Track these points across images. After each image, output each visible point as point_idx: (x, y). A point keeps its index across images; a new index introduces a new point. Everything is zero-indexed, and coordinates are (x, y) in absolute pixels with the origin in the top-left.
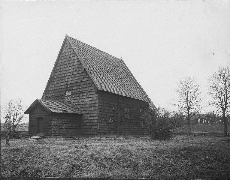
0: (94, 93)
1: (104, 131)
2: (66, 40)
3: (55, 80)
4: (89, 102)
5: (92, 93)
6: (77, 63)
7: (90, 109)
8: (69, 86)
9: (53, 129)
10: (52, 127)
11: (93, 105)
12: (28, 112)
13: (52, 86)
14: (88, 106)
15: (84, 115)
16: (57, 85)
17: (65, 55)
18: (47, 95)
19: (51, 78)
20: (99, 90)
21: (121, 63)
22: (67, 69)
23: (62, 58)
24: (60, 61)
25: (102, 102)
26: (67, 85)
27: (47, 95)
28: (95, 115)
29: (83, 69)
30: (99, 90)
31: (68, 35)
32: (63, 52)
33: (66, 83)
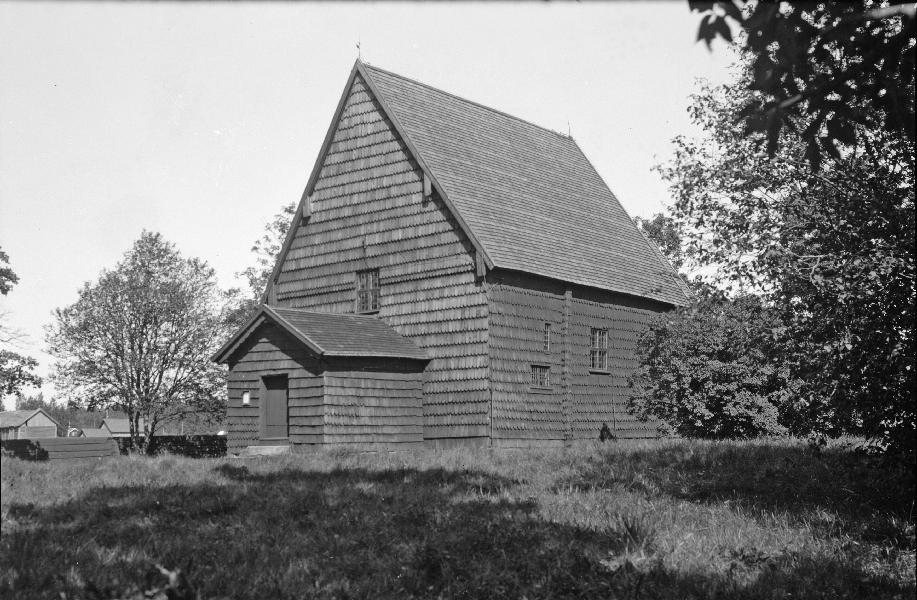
1: (515, 425)
2: (358, 75)
3: (313, 229)
4: (451, 315)
5: (464, 279)
6: (401, 167)
7: (459, 339)
8: (370, 252)
9: (326, 419)
10: (326, 409)
11: (470, 325)
12: (225, 357)
13: (301, 253)
14: (451, 327)
15: (435, 365)
16: (322, 249)
17: (352, 133)
18: (284, 289)
19: (302, 220)
20: (491, 268)
21: (570, 138)
22: (363, 186)
23: (342, 146)
24: (334, 159)
25: (501, 310)
26: (363, 248)
27: (284, 289)
28: (480, 361)
29: (428, 191)
30: (491, 268)
31: (365, 60)
32: (345, 123)
33: (358, 243)
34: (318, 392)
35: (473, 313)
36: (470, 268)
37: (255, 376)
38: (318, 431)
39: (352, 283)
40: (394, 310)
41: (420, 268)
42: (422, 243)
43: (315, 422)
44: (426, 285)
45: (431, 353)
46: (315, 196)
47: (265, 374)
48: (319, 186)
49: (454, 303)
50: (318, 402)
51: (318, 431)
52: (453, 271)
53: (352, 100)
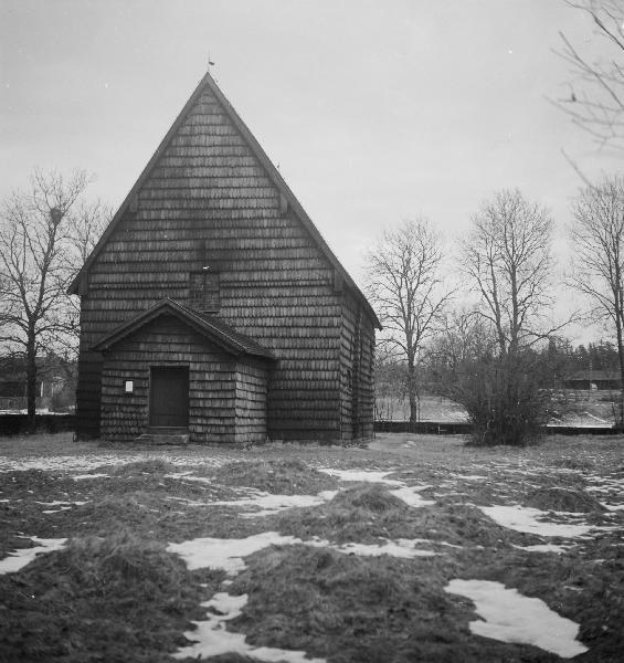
0: (326, 291)
3: (139, 225)
14: (302, 332)
34: (230, 385)
35: (326, 321)
36: (323, 282)
37: (140, 366)
38: (227, 422)
39: (185, 282)
40: (234, 312)
41: (266, 276)
42: (272, 254)
43: (223, 414)
44: (274, 292)
45: (277, 353)
46: (145, 194)
47: (157, 364)
48: (150, 185)
49: (301, 311)
50: (229, 395)
51: (227, 422)
52: (304, 283)
53: (196, 110)
